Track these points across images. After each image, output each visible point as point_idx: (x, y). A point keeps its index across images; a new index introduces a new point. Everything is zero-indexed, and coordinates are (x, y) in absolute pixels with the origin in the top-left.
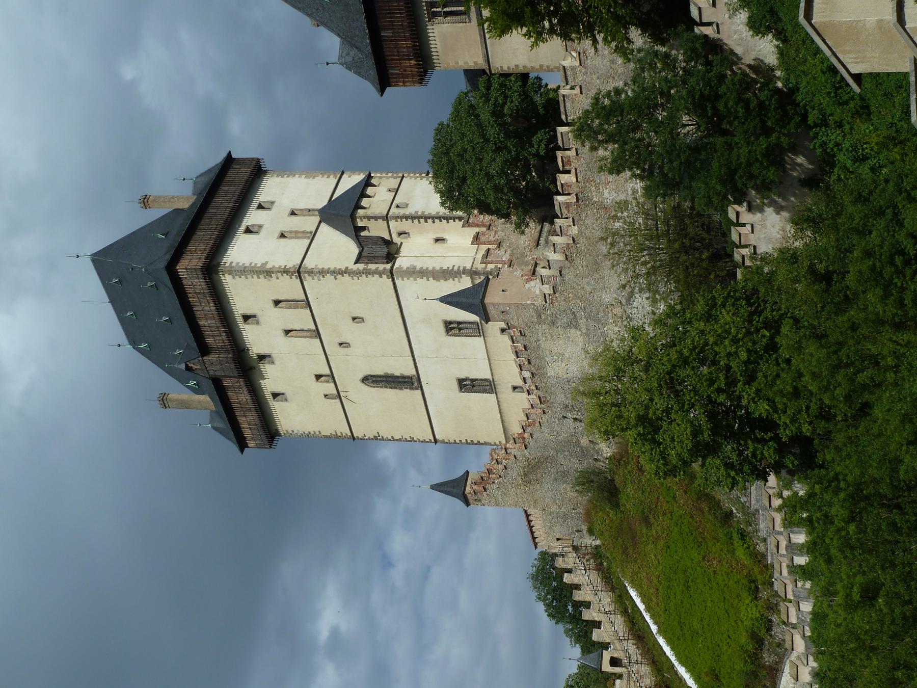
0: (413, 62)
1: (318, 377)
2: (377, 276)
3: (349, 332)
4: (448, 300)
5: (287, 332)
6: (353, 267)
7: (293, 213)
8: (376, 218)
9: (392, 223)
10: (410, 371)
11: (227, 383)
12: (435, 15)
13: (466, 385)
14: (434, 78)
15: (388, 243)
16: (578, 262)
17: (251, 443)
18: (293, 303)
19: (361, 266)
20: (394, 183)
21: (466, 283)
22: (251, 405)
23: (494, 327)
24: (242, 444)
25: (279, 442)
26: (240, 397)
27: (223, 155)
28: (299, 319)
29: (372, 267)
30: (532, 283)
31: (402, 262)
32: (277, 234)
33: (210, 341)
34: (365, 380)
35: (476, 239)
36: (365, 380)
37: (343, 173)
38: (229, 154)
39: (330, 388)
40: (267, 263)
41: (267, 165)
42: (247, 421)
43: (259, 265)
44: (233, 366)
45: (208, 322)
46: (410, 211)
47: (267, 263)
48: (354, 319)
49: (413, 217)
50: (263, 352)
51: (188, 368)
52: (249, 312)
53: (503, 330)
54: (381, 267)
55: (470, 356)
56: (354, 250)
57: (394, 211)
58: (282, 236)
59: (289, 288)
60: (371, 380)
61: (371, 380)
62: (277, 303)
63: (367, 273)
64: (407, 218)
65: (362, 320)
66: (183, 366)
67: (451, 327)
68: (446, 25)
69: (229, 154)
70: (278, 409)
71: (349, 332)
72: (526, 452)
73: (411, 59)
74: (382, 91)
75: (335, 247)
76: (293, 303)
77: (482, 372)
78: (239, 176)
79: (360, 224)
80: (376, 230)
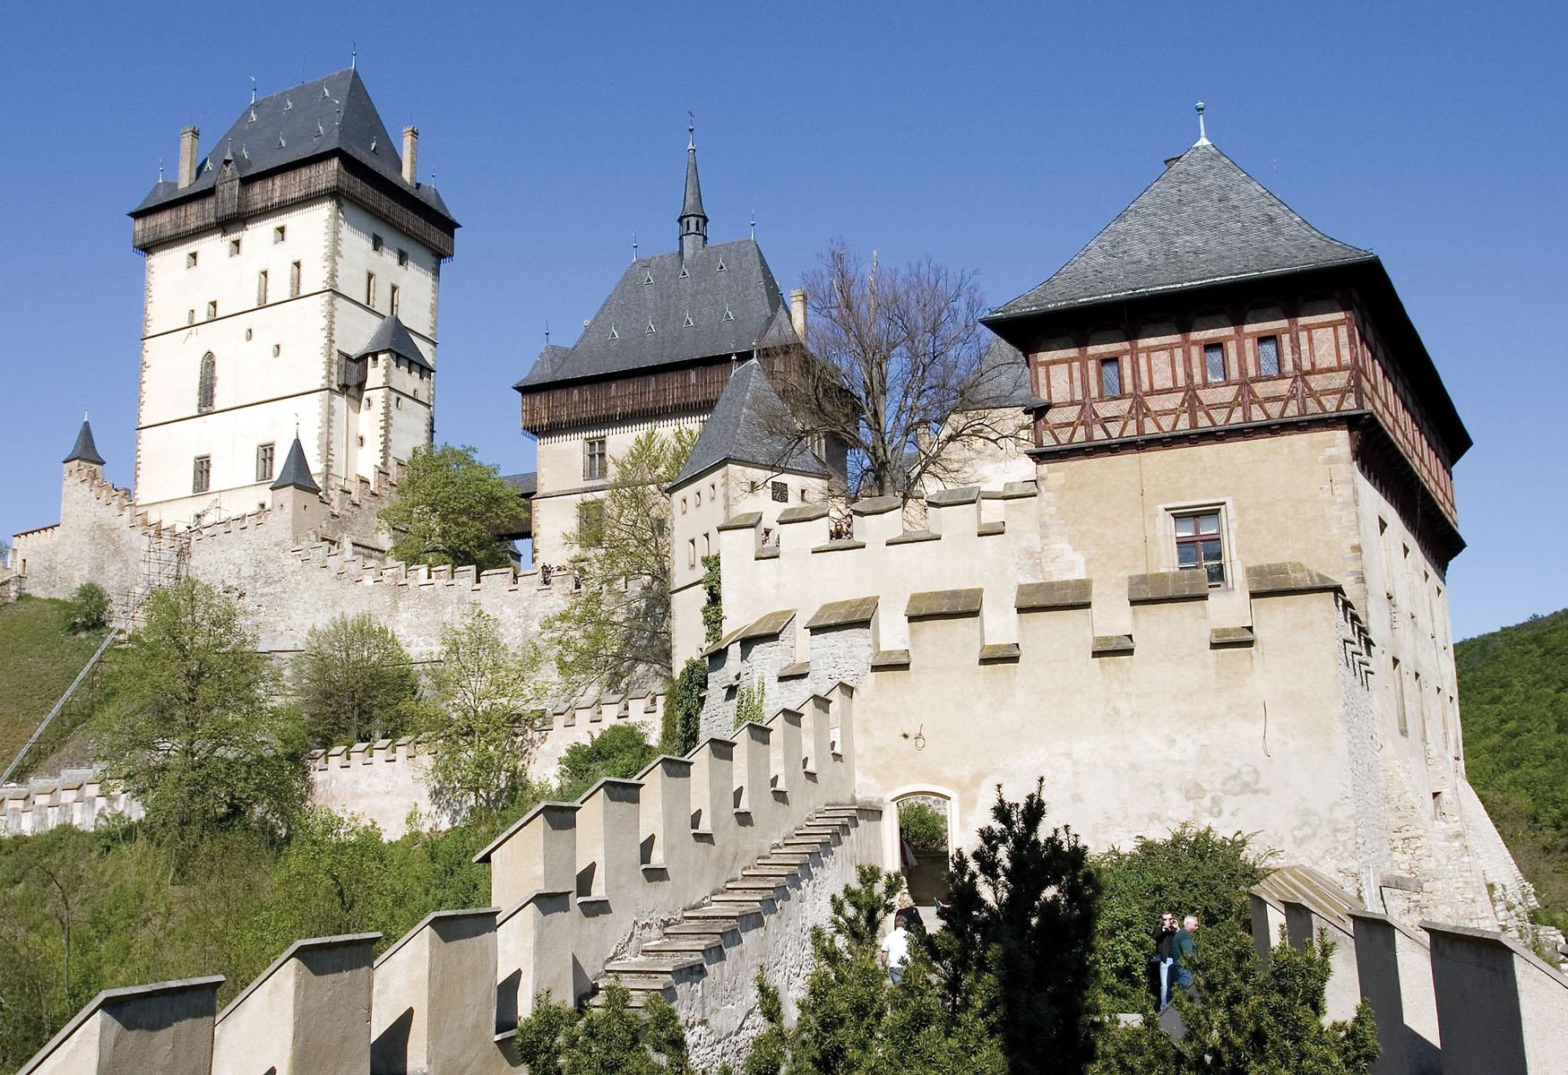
0: (545, 422)
1: (214, 304)
2: (324, 373)
3: (263, 342)
4: (297, 449)
5: (265, 273)
6: (337, 346)
7: (394, 289)
8: (387, 375)
9: (381, 392)
10: (218, 406)
11: (209, 204)
12: (592, 444)
13: (203, 467)
14: (527, 440)
15: (361, 387)
16: (337, 585)
17: (139, 225)
18: (296, 282)
19: (335, 356)
20: (423, 396)
21: (315, 466)
22: (182, 229)
23: (264, 493)
24: (137, 215)
25: (138, 256)
26: (193, 215)
27: (458, 221)
28: (279, 287)
29: (335, 369)
30: (313, 537)
31: (341, 402)
32: (373, 270)
33: (257, 188)
34: (209, 355)
35: (364, 481)
36: (209, 355)
37: (435, 344)
39: (201, 316)
41: (445, 266)
42: (165, 222)
44: (228, 212)
45: (278, 189)
46: (393, 408)
49: (387, 416)
50: (242, 245)
51: (227, 162)
52: (287, 233)
53: (263, 506)
54: (334, 378)
55: (235, 468)
56: (354, 351)
57: (395, 395)
58: (370, 276)
59: (314, 278)
60: (209, 361)
61: (209, 361)
62: (298, 264)
63: (330, 363)
64: (387, 407)
66: (228, 157)
67: (267, 451)
70: (180, 253)
71: (263, 342)
72: (125, 527)
74: (518, 389)
75: (360, 333)
76: (296, 282)
77: (216, 481)
78: (435, 236)
79: (381, 357)
80: (375, 374)
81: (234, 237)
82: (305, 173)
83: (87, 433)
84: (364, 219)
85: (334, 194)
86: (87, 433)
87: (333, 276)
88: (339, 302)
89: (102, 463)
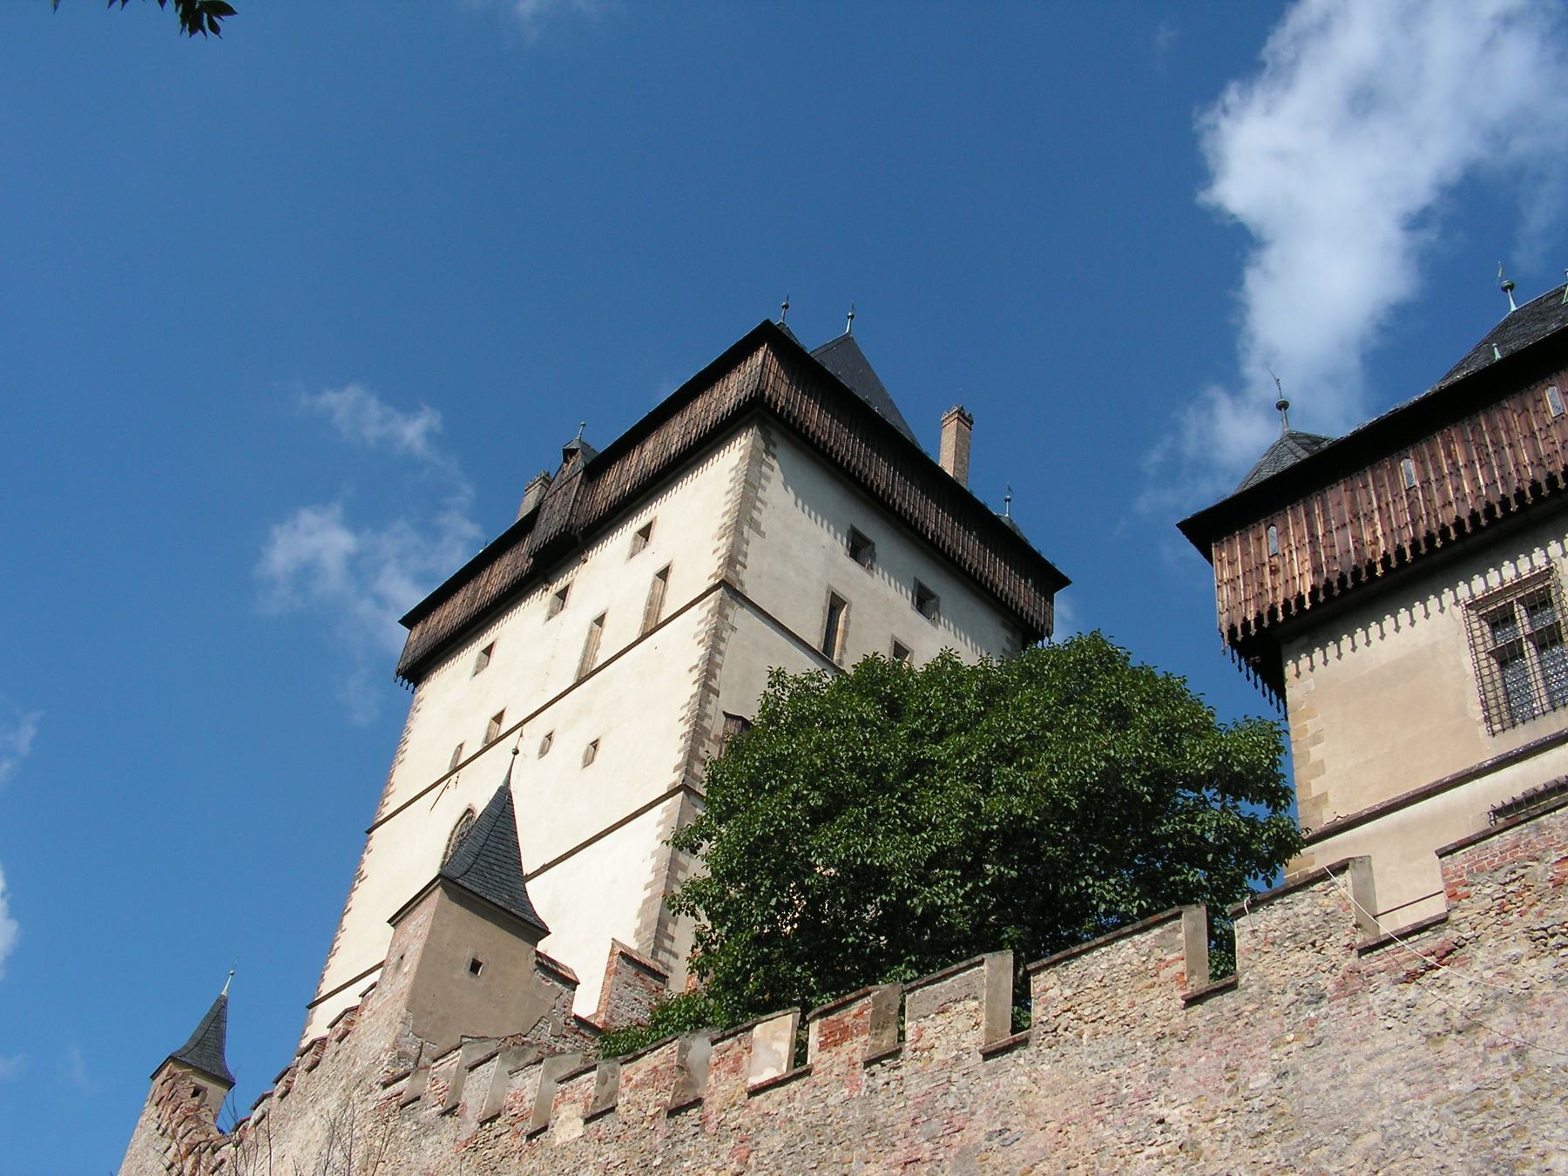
0: (1306, 585)
2: (679, 758)
3: (570, 747)
12: (1500, 620)
32: (843, 591)
38: (1063, 582)
40: (762, 534)
43: (755, 514)
47: (762, 534)
48: (595, 744)
58: (836, 604)
65: (588, 761)
68: (1467, 661)
69: (1063, 582)
71: (570, 747)
73: (1316, 570)
81: (558, 586)
82: (699, 404)
83: (217, 1017)
84: (829, 493)
85: (754, 412)
86: (217, 1017)
87: (732, 560)
88: (741, 617)
89: (229, 1083)
